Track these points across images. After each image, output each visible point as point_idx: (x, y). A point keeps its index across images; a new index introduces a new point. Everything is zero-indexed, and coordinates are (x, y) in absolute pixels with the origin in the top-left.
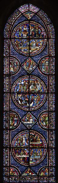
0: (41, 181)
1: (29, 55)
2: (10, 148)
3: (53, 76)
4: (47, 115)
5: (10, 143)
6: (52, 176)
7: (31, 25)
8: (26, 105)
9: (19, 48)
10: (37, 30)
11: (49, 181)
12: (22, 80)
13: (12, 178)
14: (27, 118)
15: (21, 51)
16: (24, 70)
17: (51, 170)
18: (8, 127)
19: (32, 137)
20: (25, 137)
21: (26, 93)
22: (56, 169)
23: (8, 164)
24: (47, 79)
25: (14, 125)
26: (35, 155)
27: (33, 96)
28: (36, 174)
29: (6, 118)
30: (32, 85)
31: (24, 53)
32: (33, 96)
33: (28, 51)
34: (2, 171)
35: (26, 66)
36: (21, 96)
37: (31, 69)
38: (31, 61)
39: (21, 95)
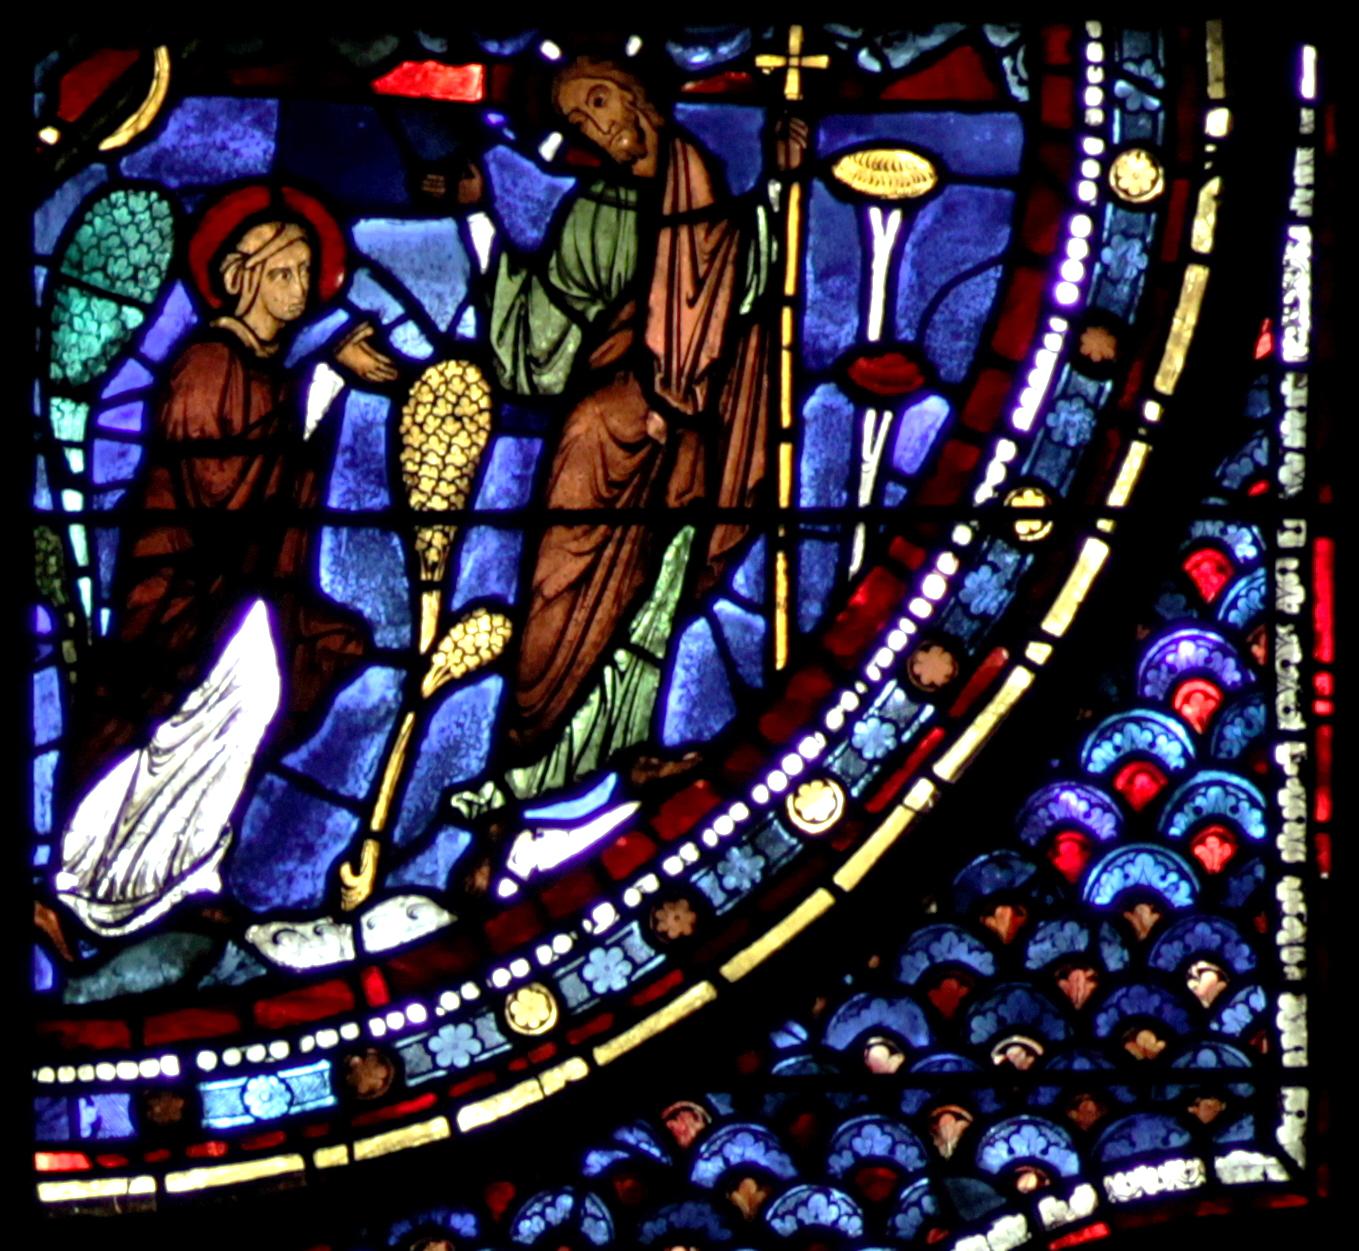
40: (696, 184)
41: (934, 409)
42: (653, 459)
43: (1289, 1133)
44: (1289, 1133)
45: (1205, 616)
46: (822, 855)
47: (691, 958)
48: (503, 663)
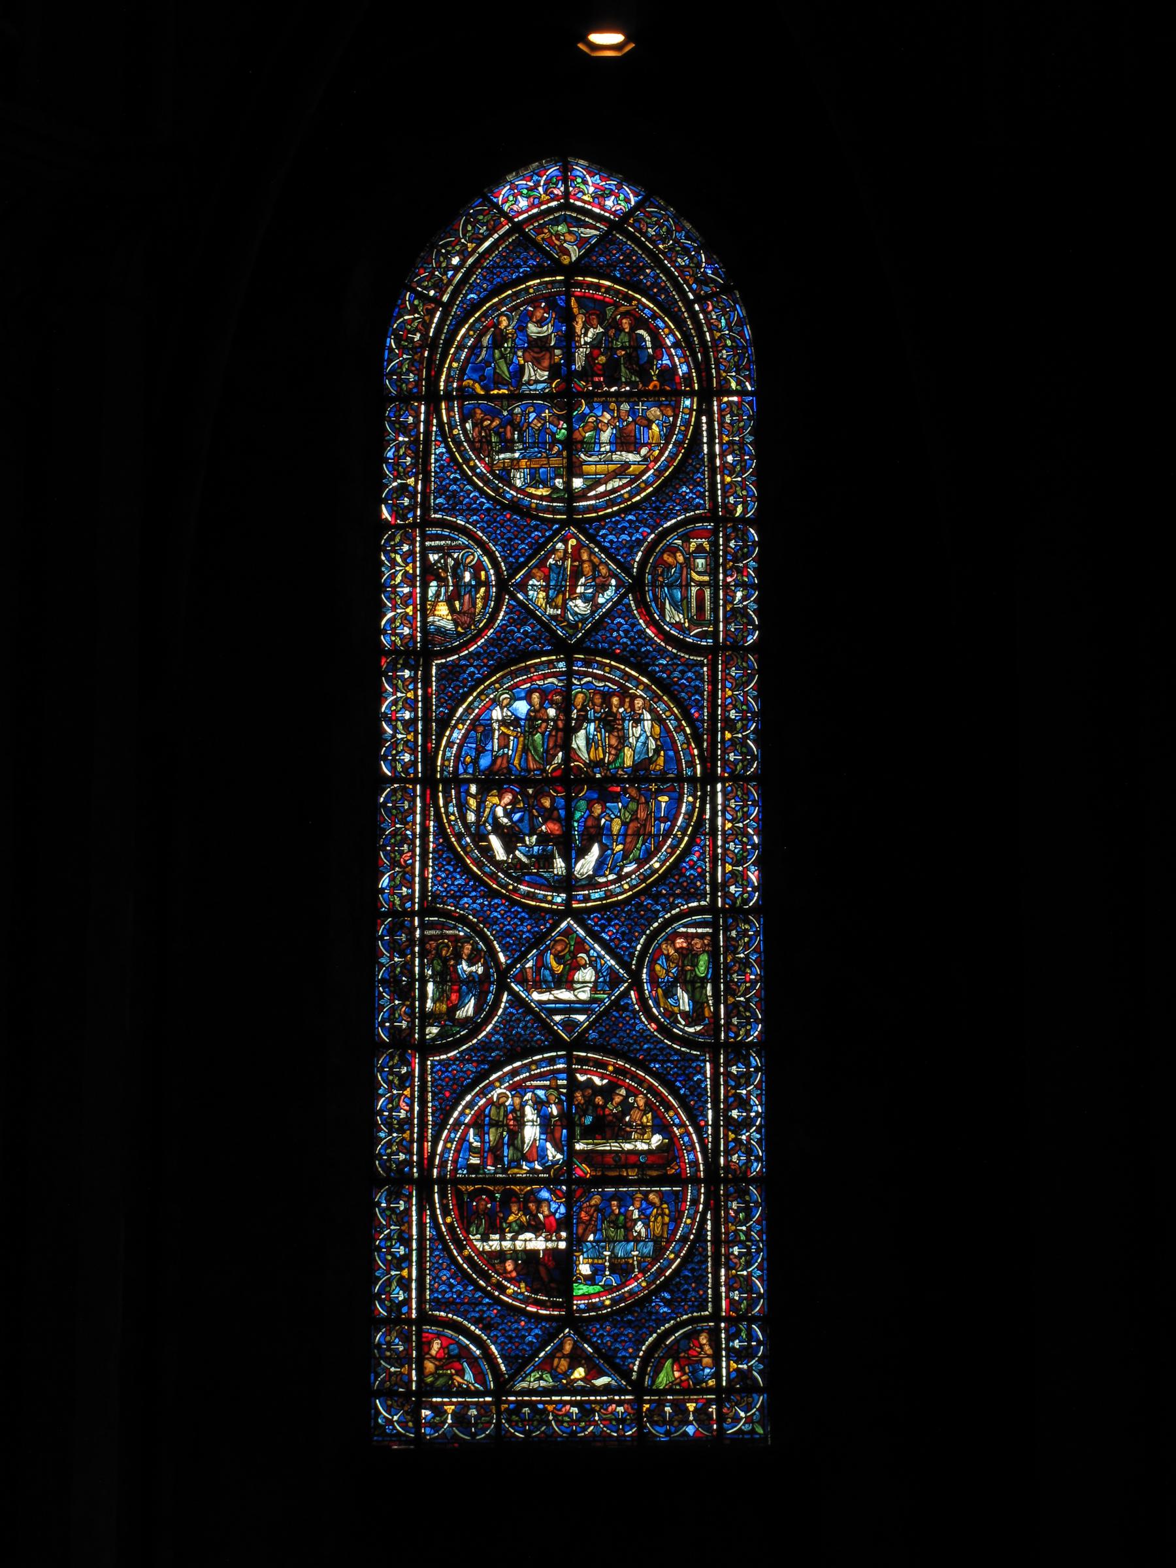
0: (659, 1432)
1: (570, 510)
2: (425, 1185)
3: (746, 660)
4: (701, 936)
5: (428, 1145)
6: (743, 1386)
7: (580, 307)
9: (490, 467)
10: (624, 338)
11: (721, 1429)
12: (517, 686)
13: (438, 1410)
14: (550, 959)
15: (512, 486)
16: (532, 614)
17: (737, 1344)
18: (411, 1028)
19: (589, 1101)
20: (539, 1104)
21: (544, 784)
24: (700, 677)
25: (461, 1014)
28: (625, 1373)
31: (532, 496)
32: (598, 801)
33: (559, 483)
34: (367, 1358)
35: (546, 589)
36: (512, 803)
37: (580, 607)
38: (585, 557)
39: (508, 798)
40: (643, 800)
46: (657, 870)
47: (643, 881)
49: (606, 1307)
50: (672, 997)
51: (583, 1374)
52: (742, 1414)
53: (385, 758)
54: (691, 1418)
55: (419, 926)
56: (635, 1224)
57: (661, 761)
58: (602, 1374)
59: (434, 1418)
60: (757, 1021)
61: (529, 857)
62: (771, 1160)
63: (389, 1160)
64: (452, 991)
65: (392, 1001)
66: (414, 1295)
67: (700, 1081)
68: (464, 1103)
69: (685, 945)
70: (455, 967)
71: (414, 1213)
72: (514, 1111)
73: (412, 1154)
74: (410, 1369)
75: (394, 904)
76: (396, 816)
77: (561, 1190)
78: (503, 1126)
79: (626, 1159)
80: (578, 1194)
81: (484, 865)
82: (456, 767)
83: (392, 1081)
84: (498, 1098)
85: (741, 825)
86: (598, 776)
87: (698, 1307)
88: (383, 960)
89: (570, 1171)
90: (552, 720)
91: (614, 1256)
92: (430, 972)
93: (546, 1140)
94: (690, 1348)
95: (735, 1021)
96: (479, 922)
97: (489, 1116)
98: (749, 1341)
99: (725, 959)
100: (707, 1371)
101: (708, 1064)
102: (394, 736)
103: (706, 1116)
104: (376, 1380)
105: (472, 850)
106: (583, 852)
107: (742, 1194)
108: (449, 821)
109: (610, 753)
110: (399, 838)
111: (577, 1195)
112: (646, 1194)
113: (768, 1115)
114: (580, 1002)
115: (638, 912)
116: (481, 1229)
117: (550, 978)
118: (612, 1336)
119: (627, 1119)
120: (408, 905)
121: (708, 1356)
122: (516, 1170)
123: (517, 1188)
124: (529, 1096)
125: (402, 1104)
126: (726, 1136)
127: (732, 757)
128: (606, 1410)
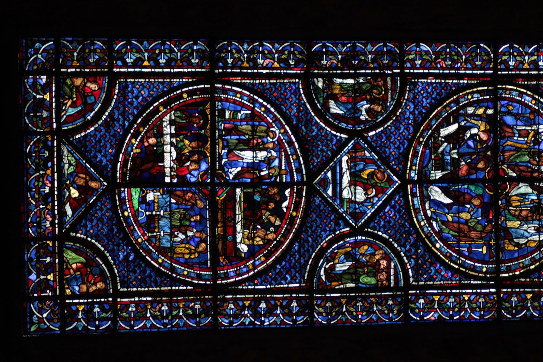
0: (32, 253)
4: (388, 279)
5: (238, 80)
6: (66, 315)
8: (437, 168)
13: (46, 88)
14: (371, 169)
17: (97, 310)
19: (271, 198)
20: (268, 161)
21: (494, 163)
22: (100, 335)
23: (125, 65)
25: (332, 103)
26: (177, 216)
27: (483, 205)
28: (74, 227)
29: (365, 54)
30: (534, 198)
34: (85, 35)
39: (484, 137)
40: (484, 235)
41: (467, 254)
42: (463, 232)
43: (414, 283)
44: (414, 283)
45: (452, 275)
48: (448, 221)
49: (123, 213)
50: (345, 258)
51: (73, 196)
52: (45, 315)
53: (511, 47)
54: (42, 277)
55: (394, 73)
56: (183, 234)
57: (511, 248)
58: (74, 211)
59: (40, 85)
60: (328, 321)
61: (442, 152)
62: (230, 332)
63: (228, 51)
64: (348, 97)
65: (341, 53)
66: (130, 70)
67: (286, 279)
68: (269, 106)
69: (382, 267)
70: (365, 99)
71: (189, 70)
72: (264, 143)
73: (232, 68)
74: (76, 67)
75: (409, 54)
76: (470, 56)
77: (207, 178)
78: (253, 135)
79: (230, 226)
80: (205, 191)
81: (437, 120)
82: (505, 99)
83: (284, 54)
84: (272, 132)
85: (467, 306)
86: (500, 202)
87: (124, 280)
88: (369, 46)
89: (221, 185)
90: (539, 169)
91: (160, 217)
92: (361, 81)
93: (242, 167)
94: (94, 276)
95: (329, 304)
96: (397, 117)
97: (260, 125)
98: (99, 319)
99: (373, 296)
100: (77, 288)
101: (298, 285)
102: (527, 53)
103: (261, 285)
104: (68, 41)
105: (447, 111)
106: (446, 192)
107: (205, 311)
108: (467, 94)
109: (516, 211)
110: (456, 58)
111: (205, 191)
112: (205, 241)
113: (262, 329)
114: (341, 191)
115: (404, 233)
116: (178, 120)
117: (357, 169)
118: (101, 218)
119: (259, 227)
120: (408, 65)
121: (88, 289)
122: (221, 145)
123: (208, 146)
124: (274, 154)
125: (267, 61)
126: (247, 299)
127: (514, 299)
128: (48, 214)
